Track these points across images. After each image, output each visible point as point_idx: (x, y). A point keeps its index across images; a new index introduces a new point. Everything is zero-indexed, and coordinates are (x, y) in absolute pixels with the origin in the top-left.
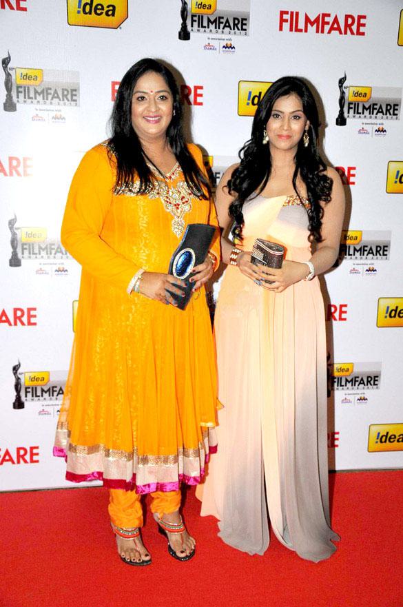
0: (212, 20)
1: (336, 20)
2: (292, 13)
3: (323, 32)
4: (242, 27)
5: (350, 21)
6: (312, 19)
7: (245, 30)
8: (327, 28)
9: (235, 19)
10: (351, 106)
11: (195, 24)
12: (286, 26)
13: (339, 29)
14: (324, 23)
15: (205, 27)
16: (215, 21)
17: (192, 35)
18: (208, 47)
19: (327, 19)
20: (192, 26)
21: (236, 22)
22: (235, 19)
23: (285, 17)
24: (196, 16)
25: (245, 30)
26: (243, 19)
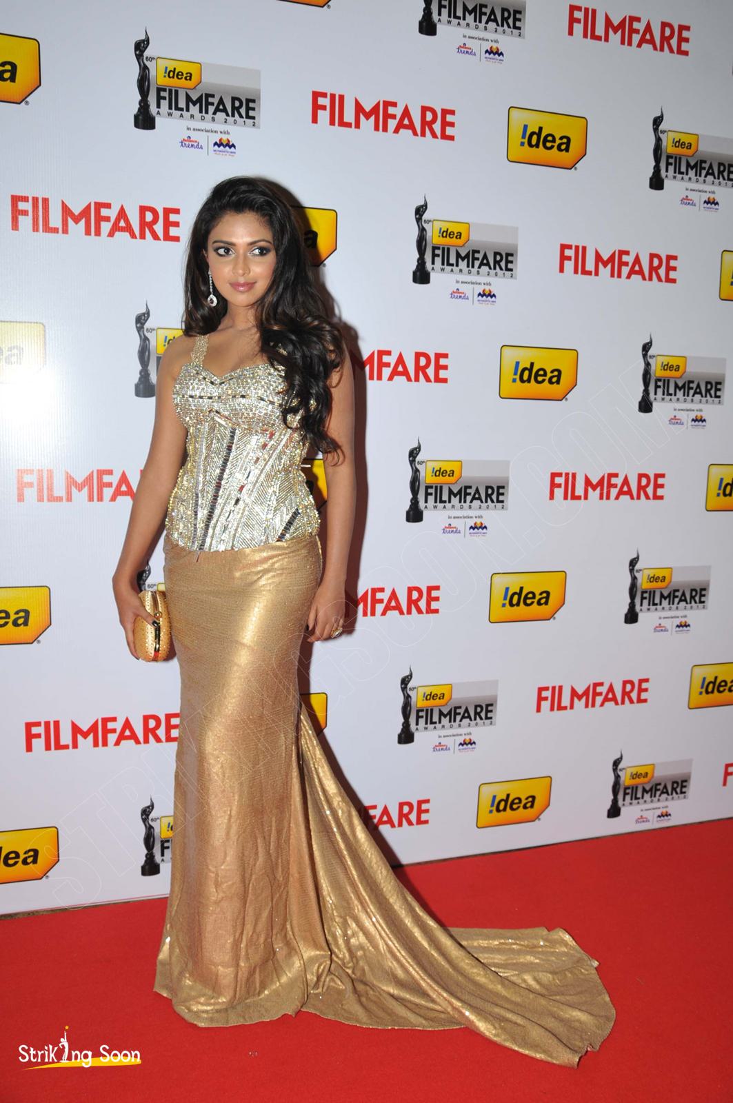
0: (463, 255)
1: (637, 260)
2: (577, 248)
3: (619, 276)
4: (506, 266)
7: (511, 270)
8: (625, 270)
9: (496, 254)
10: (659, 383)
11: (438, 260)
12: (569, 265)
13: (641, 272)
14: (622, 264)
15: (452, 265)
16: (467, 256)
17: (433, 276)
18: (457, 294)
20: (433, 263)
21: (498, 258)
22: (496, 254)
23: (568, 252)
24: (439, 248)
25: (511, 270)
26: (508, 255)
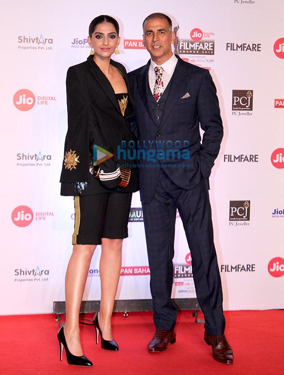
1: (249, 46)
5: (254, 46)
6: (239, 46)
8: (245, 49)
12: (229, 48)
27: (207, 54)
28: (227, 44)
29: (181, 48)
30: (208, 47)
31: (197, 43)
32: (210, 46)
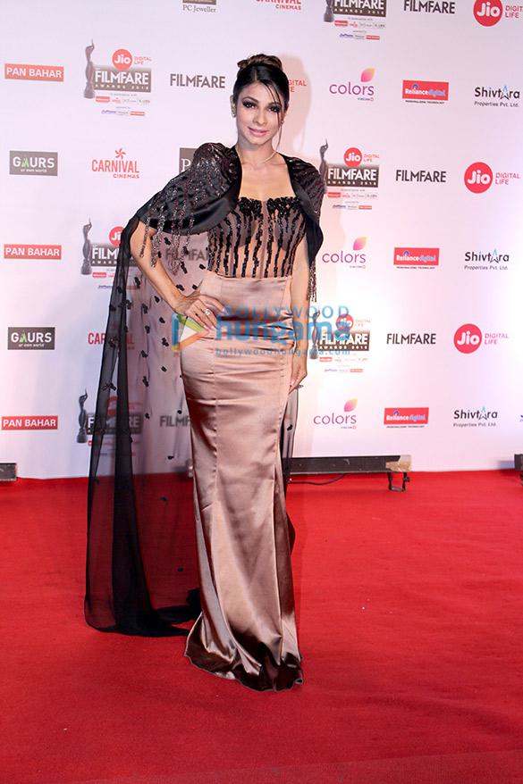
1: (206, 79)
5: (215, 80)
8: (200, 84)
13: (208, 84)
19: (200, 79)
27: (140, 90)
28: (172, 75)
29: (97, 81)
30: (141, 80)
31: (123, 73)
32: (144, 79)
